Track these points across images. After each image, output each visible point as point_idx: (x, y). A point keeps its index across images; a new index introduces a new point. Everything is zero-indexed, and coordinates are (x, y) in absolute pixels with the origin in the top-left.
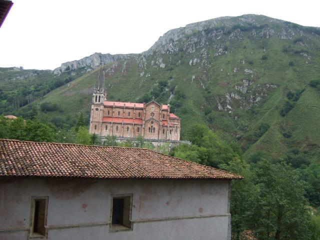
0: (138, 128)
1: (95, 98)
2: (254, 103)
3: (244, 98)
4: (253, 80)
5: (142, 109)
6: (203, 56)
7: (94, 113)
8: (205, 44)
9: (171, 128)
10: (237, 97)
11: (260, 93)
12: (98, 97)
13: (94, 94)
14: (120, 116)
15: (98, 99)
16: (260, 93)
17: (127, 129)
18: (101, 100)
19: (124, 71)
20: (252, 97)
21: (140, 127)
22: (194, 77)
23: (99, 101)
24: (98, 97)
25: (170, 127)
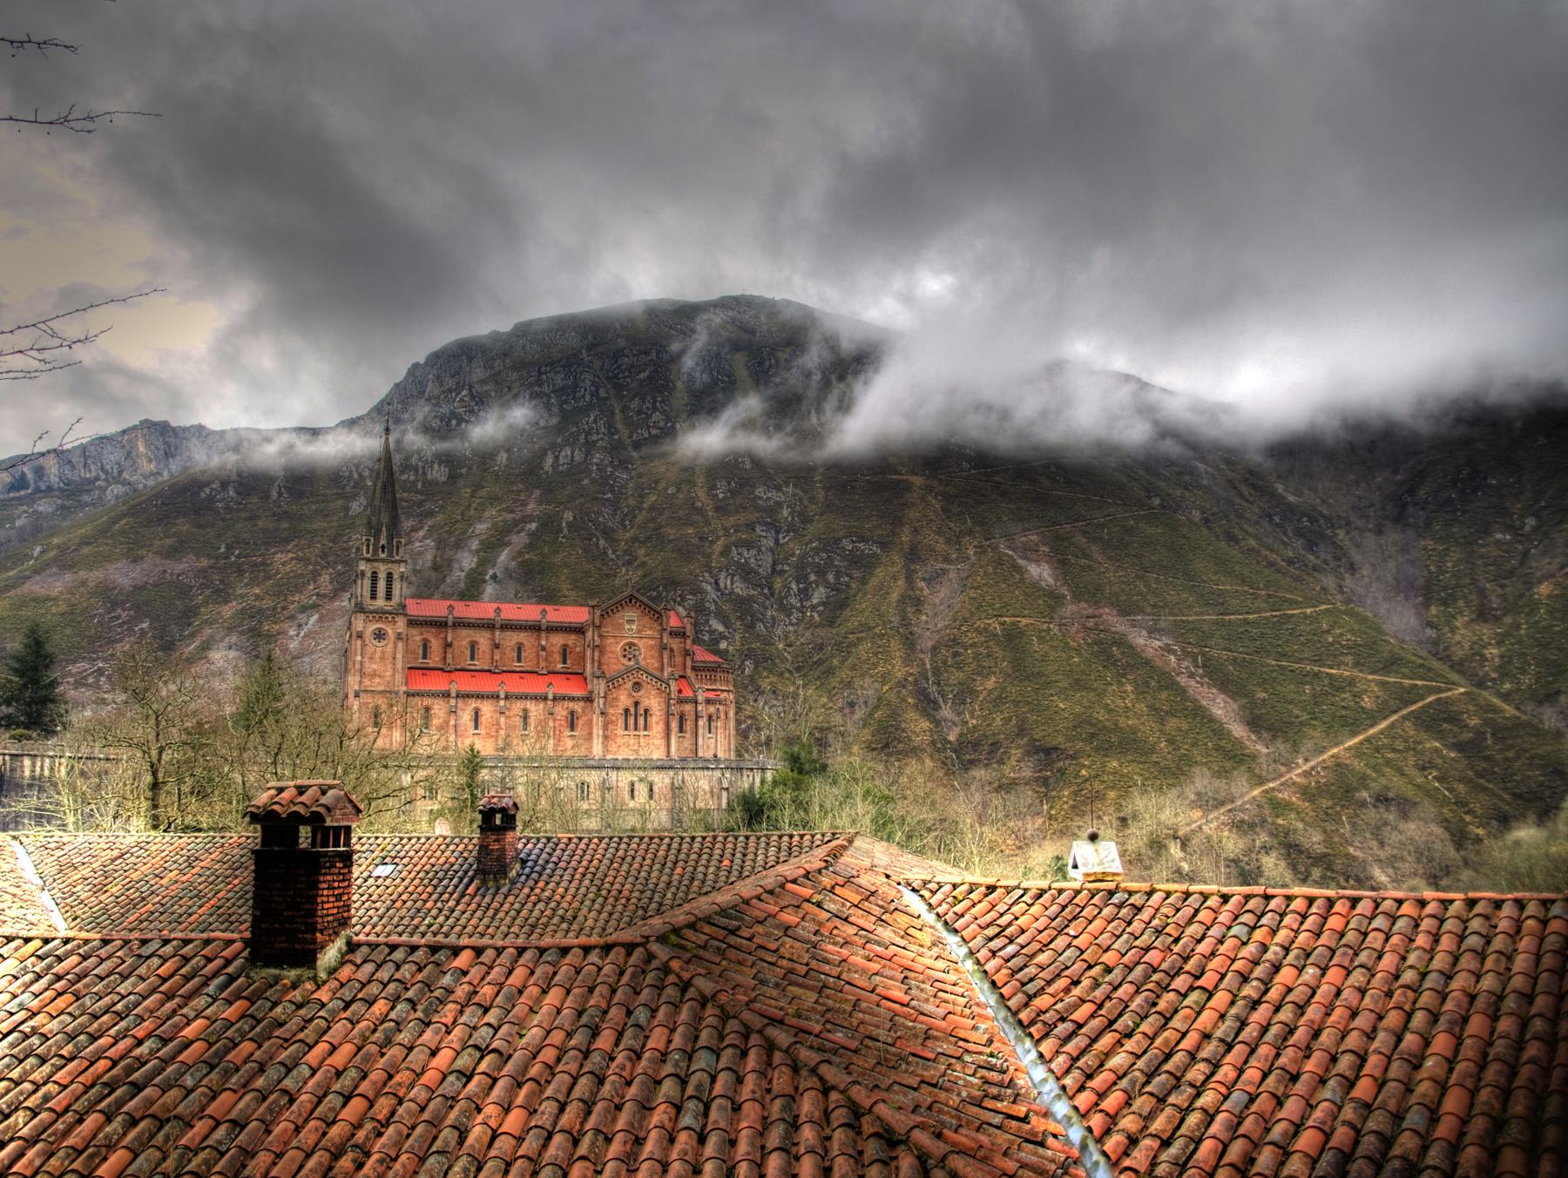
0: (572, 713)
1: (367, 583)
2: (802, 610)
3: (766, 591)
4: (791, 529)
5: (579, 630)
6: (595, 437)
7: (369, 649)
8: (595, 394)
9: (712, 709)
10: (739, 588)
11: (825, 574)
12: (382, 576)
13: (363, 566)
14: (478, 664)
15: (382, 585)
16: (821, 573)
17: (518, 721)
18: (396, 592)
19: (280, 494)
20: (794, 586)
21: (577, 707)
22: (568, 516)
23: (389, 597)
24: (382, 576)
25: (708, 702)
